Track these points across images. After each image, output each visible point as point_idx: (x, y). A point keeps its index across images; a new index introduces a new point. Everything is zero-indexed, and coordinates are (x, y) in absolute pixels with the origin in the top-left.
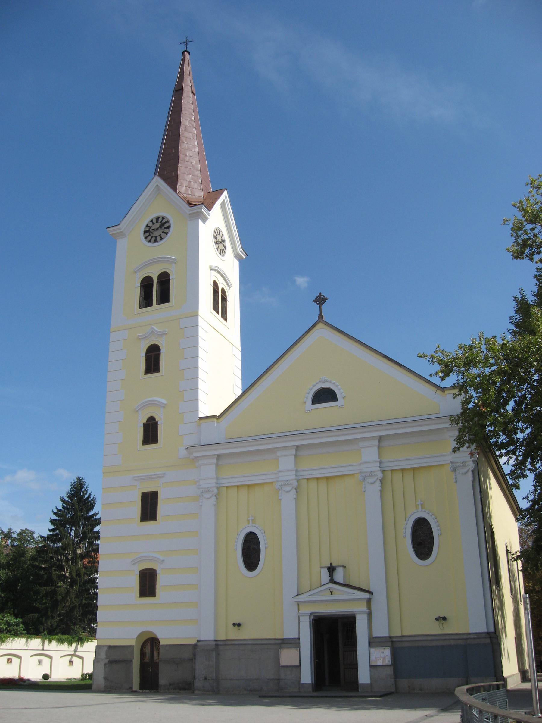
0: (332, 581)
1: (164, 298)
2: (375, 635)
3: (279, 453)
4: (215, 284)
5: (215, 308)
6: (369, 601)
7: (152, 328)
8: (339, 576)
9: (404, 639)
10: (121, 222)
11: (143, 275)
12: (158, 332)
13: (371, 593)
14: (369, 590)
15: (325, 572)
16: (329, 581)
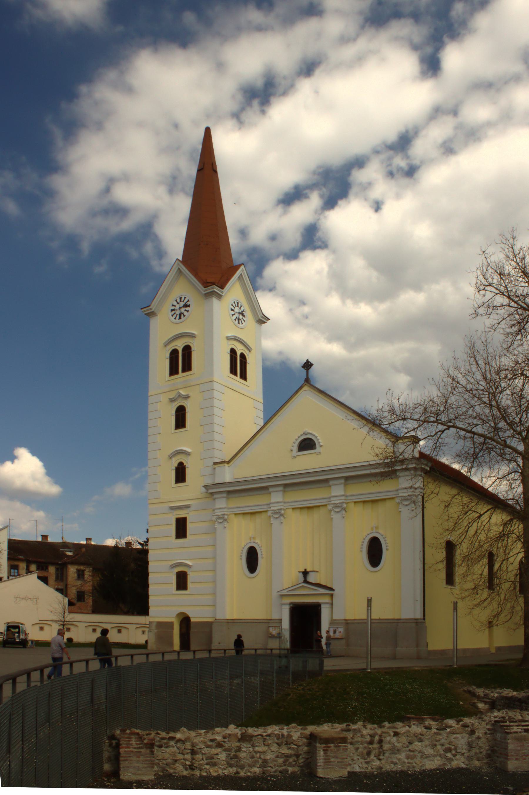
0: (306, 581)
1: (187, 367)
2: (334, 618)
3: (271, 490)
4: (233, 352)
5: (233, 371)
6: (332, 595)
7: (179, 393)
8: (311, 578)
9: (356, 621)
10: (151, 303)
11: (170, 349)
12: (184, 395)
13: (331, 589)
14: (331, 587)
15: (301, 575)
16: (302, 581)
